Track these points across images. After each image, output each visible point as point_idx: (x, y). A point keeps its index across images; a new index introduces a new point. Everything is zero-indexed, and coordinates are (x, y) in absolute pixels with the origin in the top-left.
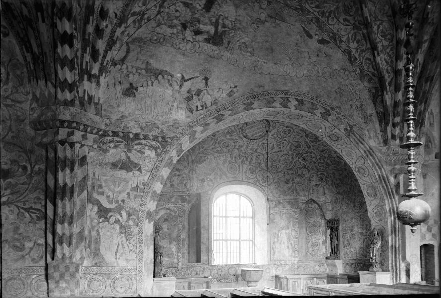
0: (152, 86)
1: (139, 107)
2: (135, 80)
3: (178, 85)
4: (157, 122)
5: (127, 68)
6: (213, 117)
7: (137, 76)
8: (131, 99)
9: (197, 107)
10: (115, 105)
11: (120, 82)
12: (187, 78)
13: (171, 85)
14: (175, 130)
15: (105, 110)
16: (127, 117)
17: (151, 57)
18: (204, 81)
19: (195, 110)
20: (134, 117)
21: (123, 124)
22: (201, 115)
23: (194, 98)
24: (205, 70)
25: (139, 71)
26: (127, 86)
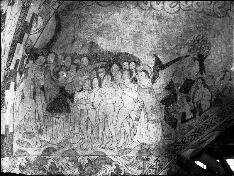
0: (100, 86)
1: (77, 130)
2: (69, 81)
3: (149, 77)
4: (108, 153)
5: (56, 59)
6: (213, 128)
7: (73, 72)
8: (62, 116)
9: (184, 114)
10: (35, 131)
11: (43, 89)
12: (164, 61)
13: (135, 80)
14: (141, 163)
15: (19, 142)
16: (55, 150)
17: (99, 32)
18: (197, 62)
19: (180, 121)
20: (67, 148)
21: (49, 164)
22: (190, 128)
23: (179, 98)
24: (198, 42)
25: (77, 61)
26: (55, 93)
